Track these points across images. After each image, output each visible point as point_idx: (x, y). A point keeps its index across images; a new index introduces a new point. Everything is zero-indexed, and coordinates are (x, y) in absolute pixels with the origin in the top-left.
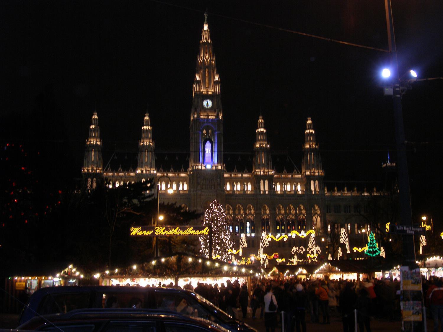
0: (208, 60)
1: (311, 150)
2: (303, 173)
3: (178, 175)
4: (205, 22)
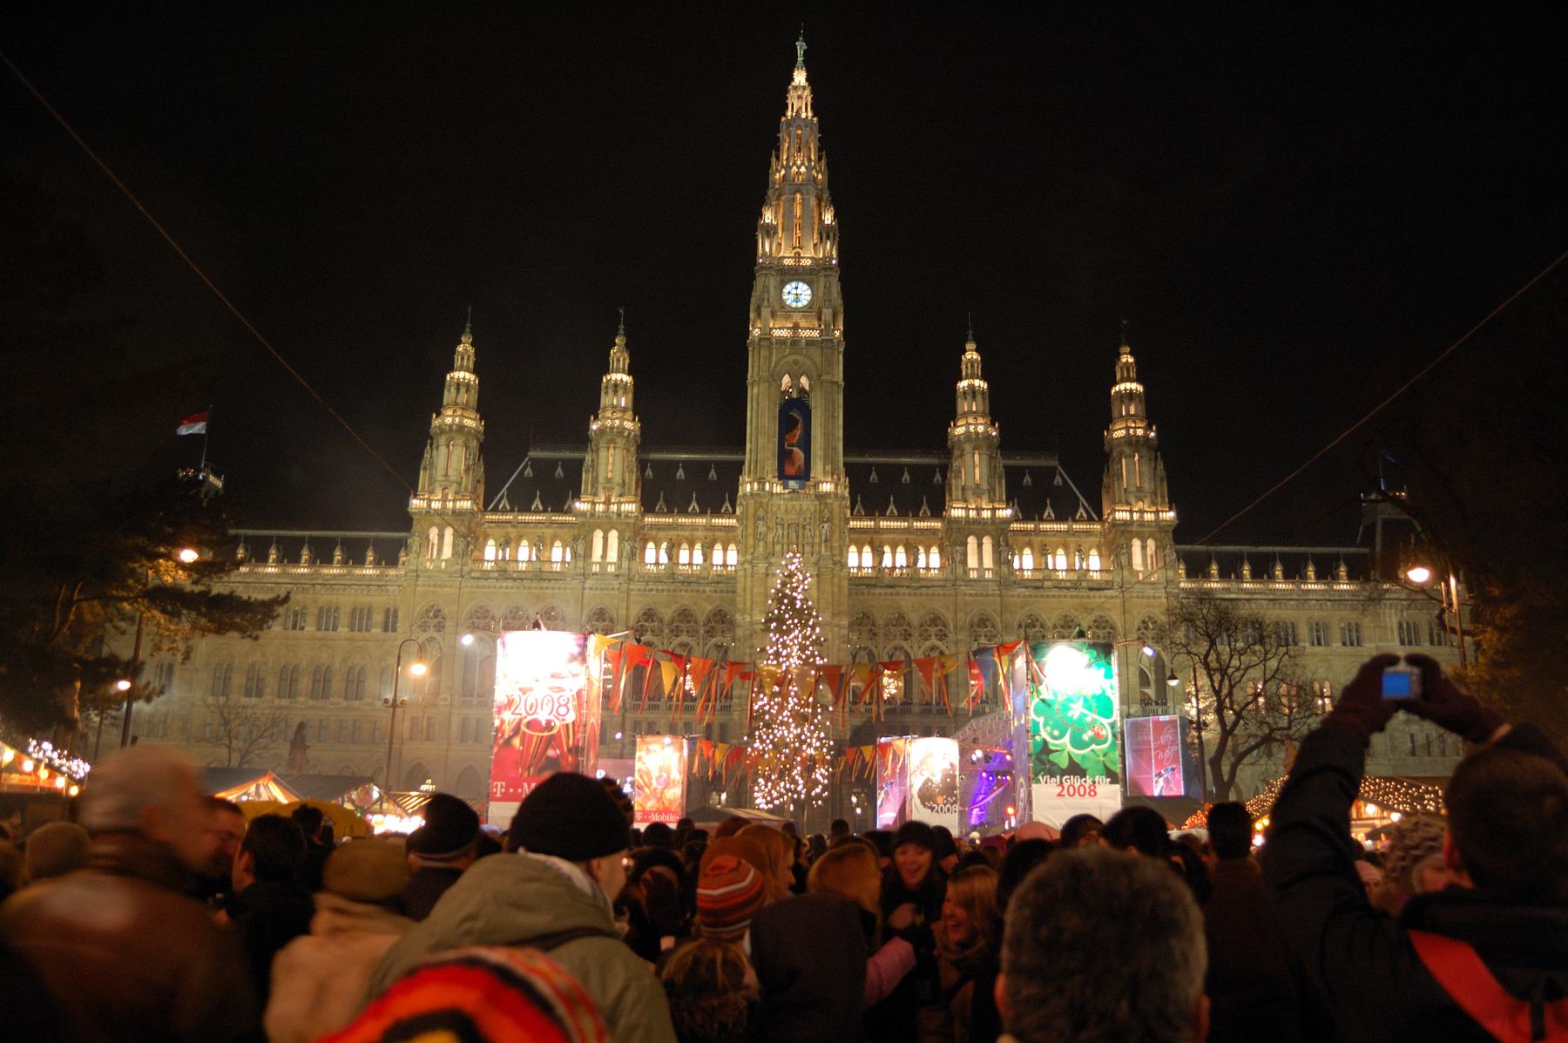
0: (803, 169)
1: (1130, 441)
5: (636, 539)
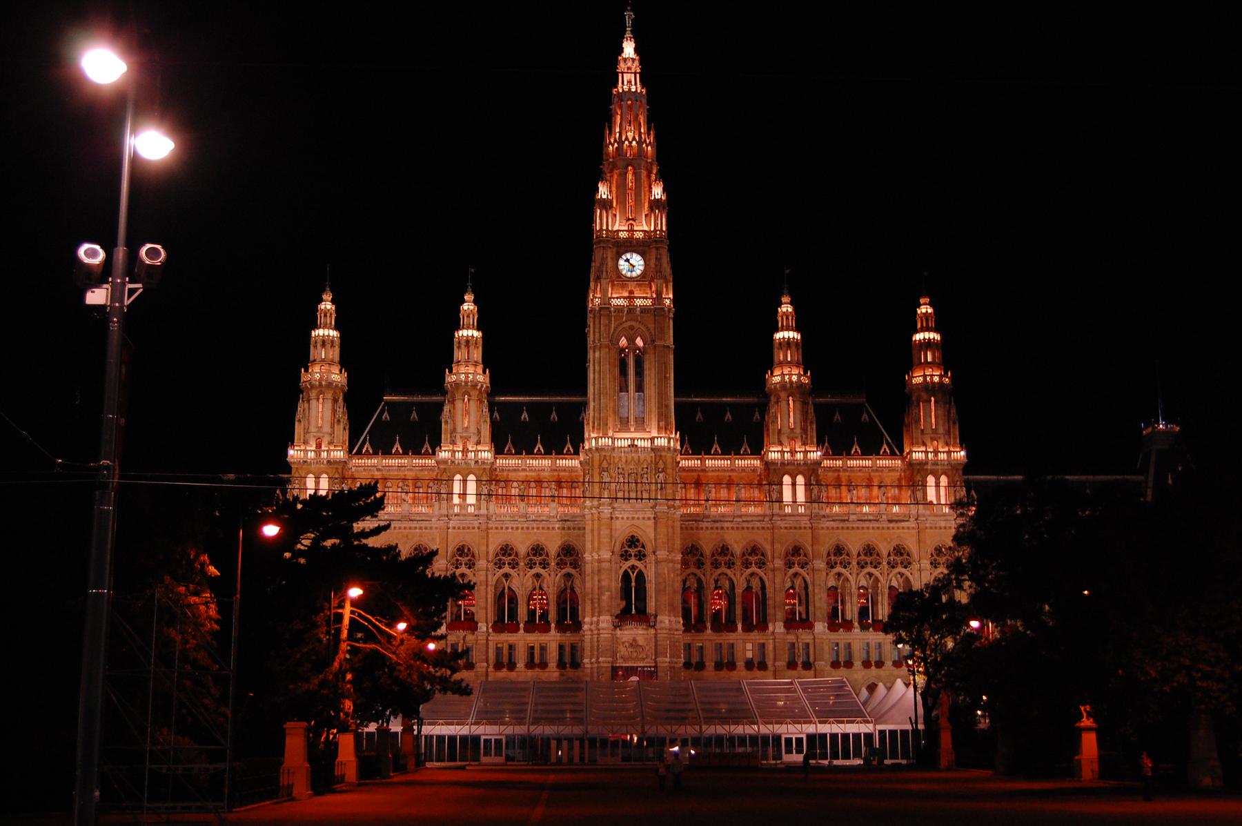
1: (929, 388)
3: (554, 463)
4: (628, 35)
5: (492, 481)
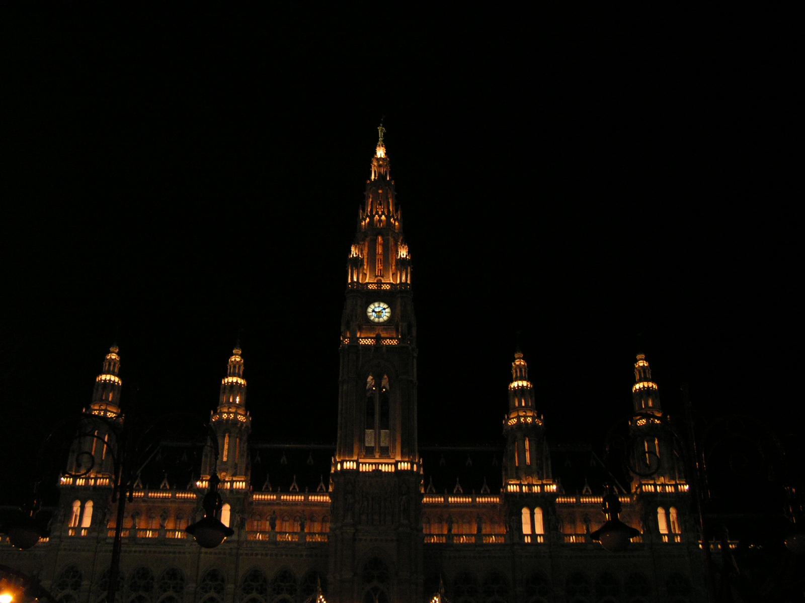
0: (383, 217)
2: (634, 490)
3: (306, 499)
